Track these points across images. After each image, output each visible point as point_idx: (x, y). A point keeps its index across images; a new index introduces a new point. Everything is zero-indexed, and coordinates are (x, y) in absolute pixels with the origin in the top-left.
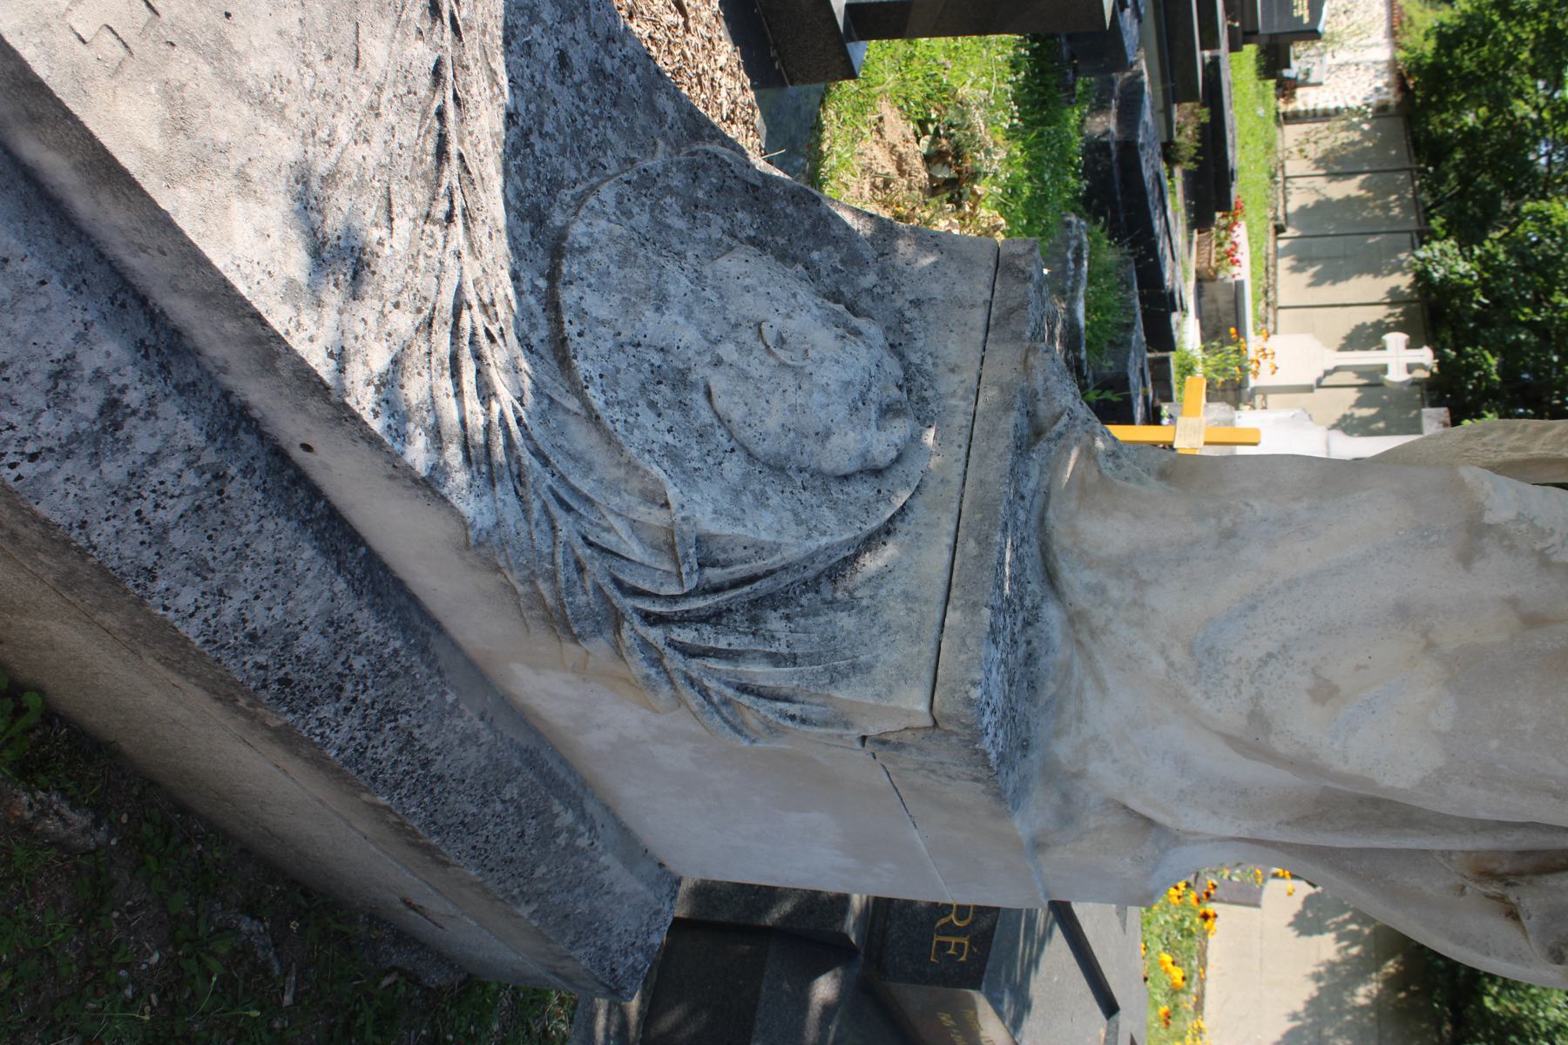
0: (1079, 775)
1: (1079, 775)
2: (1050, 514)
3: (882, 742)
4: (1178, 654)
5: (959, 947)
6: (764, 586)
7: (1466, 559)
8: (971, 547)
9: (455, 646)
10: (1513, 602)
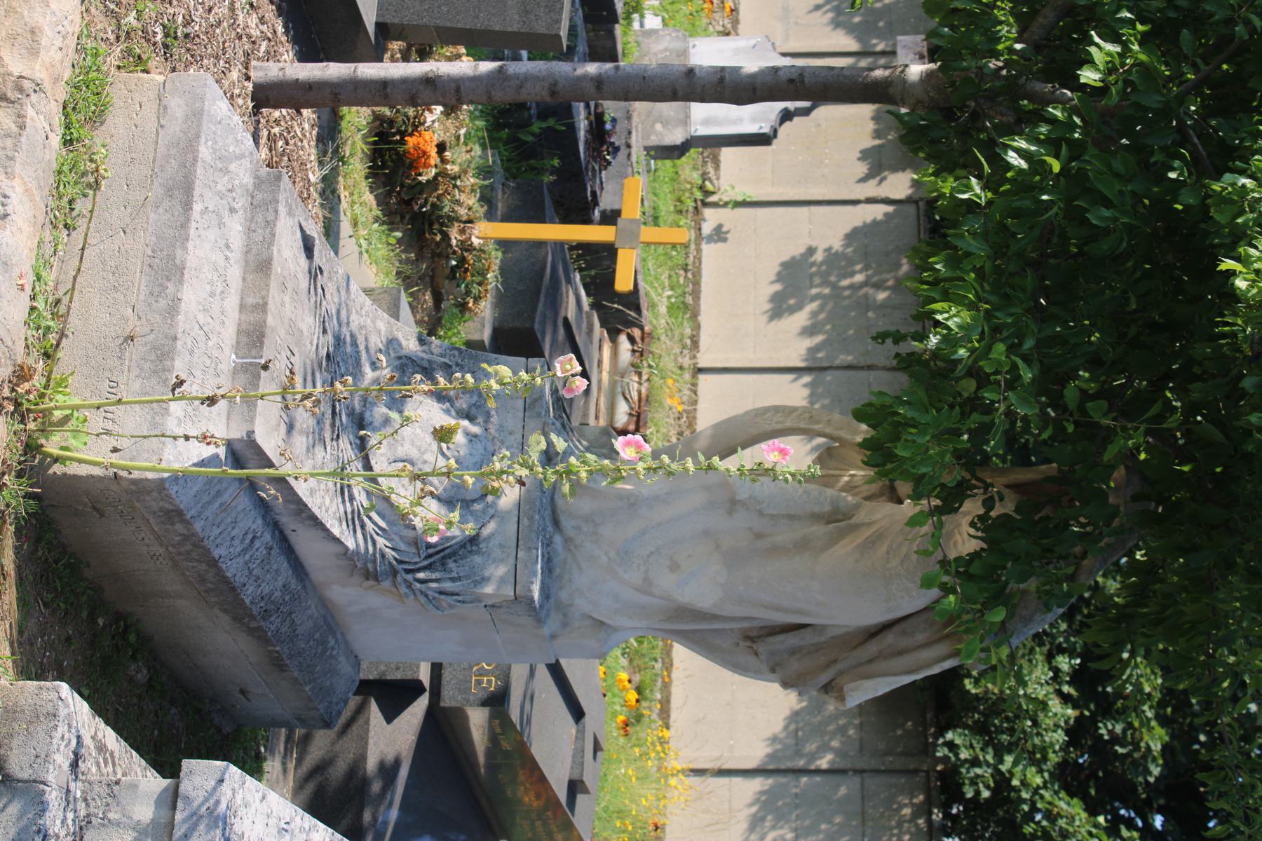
0: (570, 605)
1: (570, 605)
2: (556, 497)
3: (493, 606)
4: (613, 555)
5: (489, 682)
6: (446, 552)
7: (730, 513)
8: (525, 521)
9: (310, 581)
10: (750, 529)
